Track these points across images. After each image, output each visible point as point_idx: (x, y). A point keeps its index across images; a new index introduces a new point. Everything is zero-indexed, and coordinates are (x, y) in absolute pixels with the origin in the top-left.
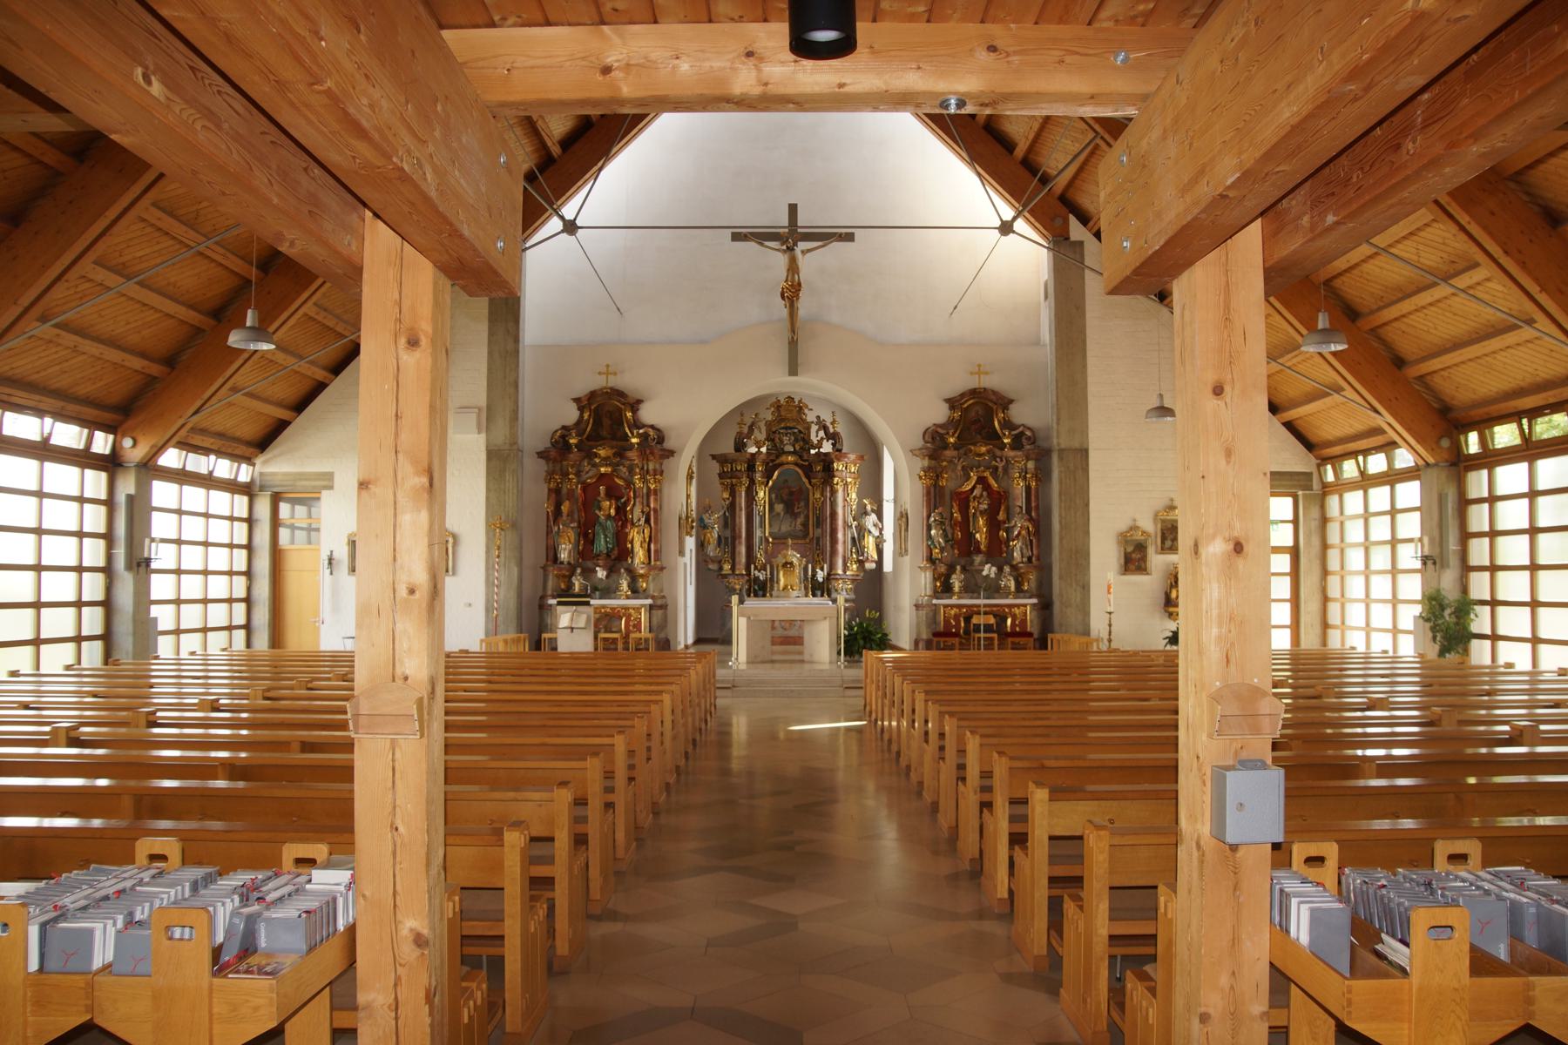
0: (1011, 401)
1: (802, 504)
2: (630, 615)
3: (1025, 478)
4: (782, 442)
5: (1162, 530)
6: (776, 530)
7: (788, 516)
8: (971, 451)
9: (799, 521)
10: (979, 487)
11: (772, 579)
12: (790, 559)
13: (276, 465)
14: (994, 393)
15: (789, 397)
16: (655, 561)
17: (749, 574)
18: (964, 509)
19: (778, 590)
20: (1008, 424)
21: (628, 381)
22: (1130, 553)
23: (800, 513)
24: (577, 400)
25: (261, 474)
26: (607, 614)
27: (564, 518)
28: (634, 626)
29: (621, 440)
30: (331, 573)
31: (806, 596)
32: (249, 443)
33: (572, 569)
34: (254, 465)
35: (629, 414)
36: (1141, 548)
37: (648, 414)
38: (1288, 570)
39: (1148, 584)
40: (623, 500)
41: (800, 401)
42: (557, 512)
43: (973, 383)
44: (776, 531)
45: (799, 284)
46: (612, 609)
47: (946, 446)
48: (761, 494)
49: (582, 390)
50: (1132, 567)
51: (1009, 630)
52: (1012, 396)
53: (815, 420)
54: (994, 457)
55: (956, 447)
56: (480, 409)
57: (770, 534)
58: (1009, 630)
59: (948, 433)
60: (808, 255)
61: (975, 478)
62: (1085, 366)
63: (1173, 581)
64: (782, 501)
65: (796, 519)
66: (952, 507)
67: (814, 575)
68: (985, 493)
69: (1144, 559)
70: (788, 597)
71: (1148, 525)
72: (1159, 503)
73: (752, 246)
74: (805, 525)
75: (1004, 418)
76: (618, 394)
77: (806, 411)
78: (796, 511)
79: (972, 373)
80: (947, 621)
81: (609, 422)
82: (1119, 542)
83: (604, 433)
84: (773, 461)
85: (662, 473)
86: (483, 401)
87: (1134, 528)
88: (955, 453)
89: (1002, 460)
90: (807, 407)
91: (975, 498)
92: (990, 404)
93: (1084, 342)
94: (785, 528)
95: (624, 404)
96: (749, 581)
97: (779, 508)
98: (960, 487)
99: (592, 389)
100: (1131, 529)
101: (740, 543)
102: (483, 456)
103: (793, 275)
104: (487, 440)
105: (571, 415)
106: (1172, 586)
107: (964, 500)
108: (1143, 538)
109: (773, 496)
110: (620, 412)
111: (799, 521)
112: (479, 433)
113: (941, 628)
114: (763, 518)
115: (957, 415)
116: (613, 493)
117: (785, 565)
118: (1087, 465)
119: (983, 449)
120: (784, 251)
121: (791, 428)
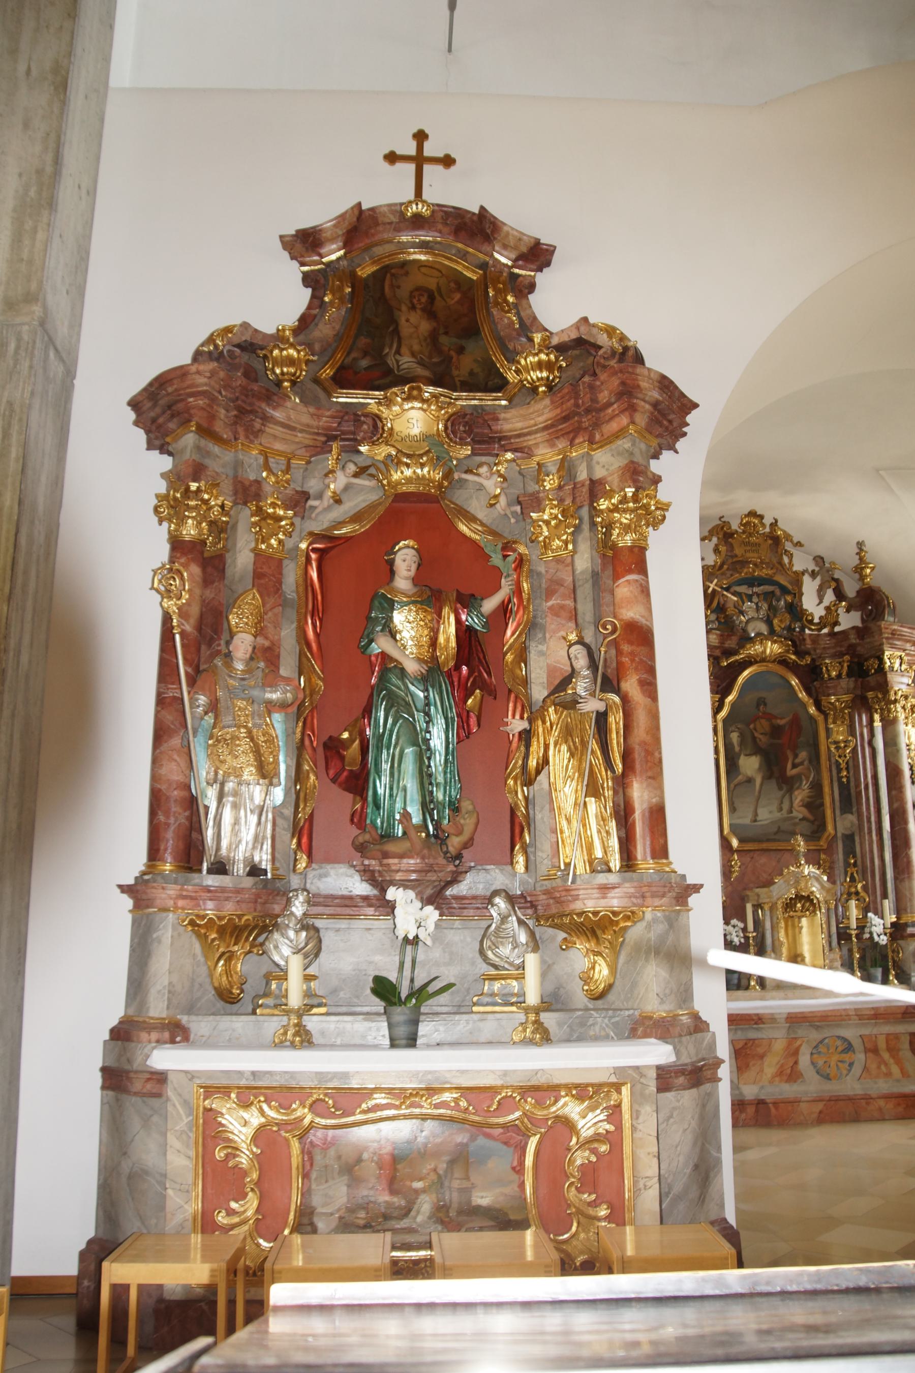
1: (803, 755)
7: (773, 784)
9: (801, 795)
15: (752, 514)
23: (798, 777)
29: (469, 386)
41: (774, 524)
44: (747, 821)
53: (812, 566)
57: (731, 825)
64: (757, 750)
65: (790, 791)
67: (862, 926)
74: (815, 805)
77: (788, 546)
78: (791, 772)
81: (425, 326)
90: (788, 537)
94: (768, 814)
97: (750, 765)
109: (735, 737)
117: (789, 905)
121: (761, 581)
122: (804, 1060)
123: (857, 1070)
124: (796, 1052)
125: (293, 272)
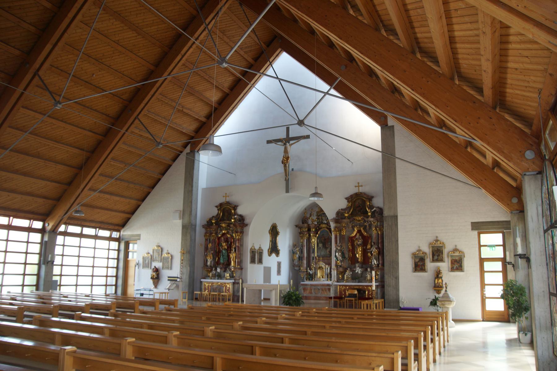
0: (372, 197)
2: (226, 286)
3: (376, 230)
4: (322, 220)
5: (432, 251)
6: (319, 254)
8: (354, 219)
9: (328, 250)
10: (358, 234)
11: (315, 273)
12: (321, 265)
13: (126, 233)
14: (365, 194)
16: (237, 265)
17: (307, 272)
18: (353, 245)
19: (317, 278)
20: (371, 207)
21: (234, 199)
22: (417, 262)
23: (328, 247)
24: (217, 207)
25: (123, 235)
26: (219, 285)
27: (209, 250)
28: (228, 290)
30: (138, 268)
31: (328, 280)
32: (118, 225)
33: (211, 267)
34: (120, 232)
35: (233, 211)
36: (422, 260)
37: (240, 211)
38: (501, 269)
39: (427, 276)
40: (229, 243)
42: (206, 249)
43: (355, 190)
45: (288, 157)
46: (221, 284)
47: (345, 218)
48: (314, 240)
49: (217, 204)
50: (418, 269)
51: (367, 297)
52: (373, 195)
54: (365, 221)
55: (349, 218)
56: (180, 211)
57: (317, 255)
58: (367, 297)
59: (345, 212)
60: (292, 146)
61: (357, 230)
62: (395, 179)
63: (438, 274)
64: (322, 243)
66: (348, 244)
68: (360, 237)
69: (424, 265)
70: (320, 280)
71: (426, 249)
72: (431, 239)
73: (273, 145)
75: (370, 205)
76: (228, 203)
78: (327, 246)
79: (356, 186)
80: (340, 292)
82: (412, 258)
83: (225, 218)
84: (318, 227)
85: (243, 232)
86: (181, 209)
87: (419, 250)
88: (348, 220)
89: (368, 223)
91: (356, 239)
92: (364, 199)
93: (395, 169)
94: (323, 253)
95: (231, 207)
96: (307, 274)
97: (321, 245)
98: (351, 234)
99: (221, 203)
100: (417, 251)
101: (304, 259)
102: (181, 228)
103: (286, 154)
104: (182, 222)
105: (215, 212)
106: (435, 278)
107: (352, 240)
108: (423, 255)
109: (318, 241)
110: (230, 210)
111: (328, 250)
112: (180, 219)
113: (338, 295)
114: (314, 250)
115: (350, 204)
116: (227, 241)
118: (397, 223)
119: (360, 218)
120: (283, 145)
122: (313, 291)
123: (320, 293)
124: (312, 290)
125: (216, 209)
